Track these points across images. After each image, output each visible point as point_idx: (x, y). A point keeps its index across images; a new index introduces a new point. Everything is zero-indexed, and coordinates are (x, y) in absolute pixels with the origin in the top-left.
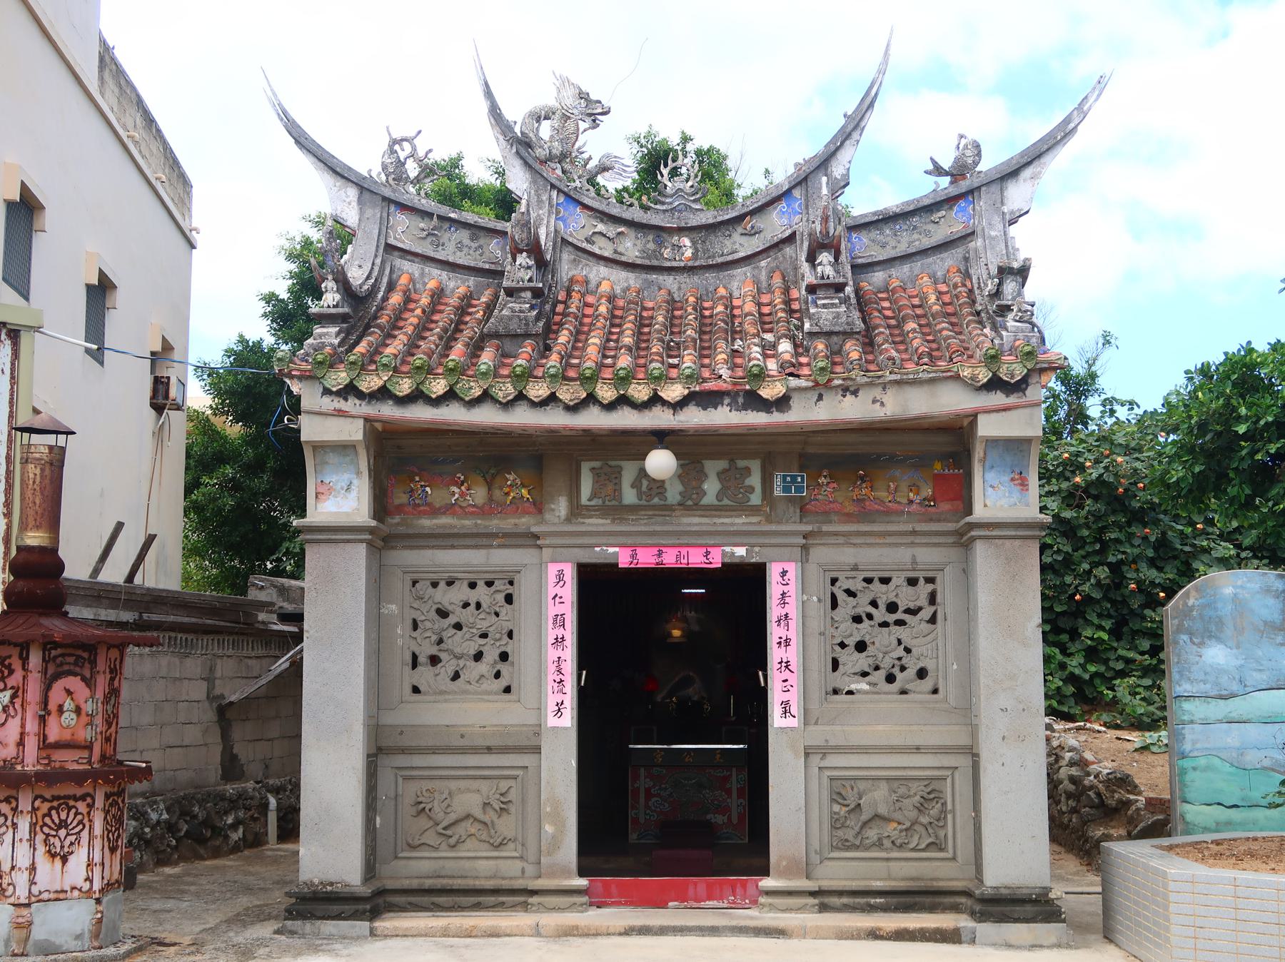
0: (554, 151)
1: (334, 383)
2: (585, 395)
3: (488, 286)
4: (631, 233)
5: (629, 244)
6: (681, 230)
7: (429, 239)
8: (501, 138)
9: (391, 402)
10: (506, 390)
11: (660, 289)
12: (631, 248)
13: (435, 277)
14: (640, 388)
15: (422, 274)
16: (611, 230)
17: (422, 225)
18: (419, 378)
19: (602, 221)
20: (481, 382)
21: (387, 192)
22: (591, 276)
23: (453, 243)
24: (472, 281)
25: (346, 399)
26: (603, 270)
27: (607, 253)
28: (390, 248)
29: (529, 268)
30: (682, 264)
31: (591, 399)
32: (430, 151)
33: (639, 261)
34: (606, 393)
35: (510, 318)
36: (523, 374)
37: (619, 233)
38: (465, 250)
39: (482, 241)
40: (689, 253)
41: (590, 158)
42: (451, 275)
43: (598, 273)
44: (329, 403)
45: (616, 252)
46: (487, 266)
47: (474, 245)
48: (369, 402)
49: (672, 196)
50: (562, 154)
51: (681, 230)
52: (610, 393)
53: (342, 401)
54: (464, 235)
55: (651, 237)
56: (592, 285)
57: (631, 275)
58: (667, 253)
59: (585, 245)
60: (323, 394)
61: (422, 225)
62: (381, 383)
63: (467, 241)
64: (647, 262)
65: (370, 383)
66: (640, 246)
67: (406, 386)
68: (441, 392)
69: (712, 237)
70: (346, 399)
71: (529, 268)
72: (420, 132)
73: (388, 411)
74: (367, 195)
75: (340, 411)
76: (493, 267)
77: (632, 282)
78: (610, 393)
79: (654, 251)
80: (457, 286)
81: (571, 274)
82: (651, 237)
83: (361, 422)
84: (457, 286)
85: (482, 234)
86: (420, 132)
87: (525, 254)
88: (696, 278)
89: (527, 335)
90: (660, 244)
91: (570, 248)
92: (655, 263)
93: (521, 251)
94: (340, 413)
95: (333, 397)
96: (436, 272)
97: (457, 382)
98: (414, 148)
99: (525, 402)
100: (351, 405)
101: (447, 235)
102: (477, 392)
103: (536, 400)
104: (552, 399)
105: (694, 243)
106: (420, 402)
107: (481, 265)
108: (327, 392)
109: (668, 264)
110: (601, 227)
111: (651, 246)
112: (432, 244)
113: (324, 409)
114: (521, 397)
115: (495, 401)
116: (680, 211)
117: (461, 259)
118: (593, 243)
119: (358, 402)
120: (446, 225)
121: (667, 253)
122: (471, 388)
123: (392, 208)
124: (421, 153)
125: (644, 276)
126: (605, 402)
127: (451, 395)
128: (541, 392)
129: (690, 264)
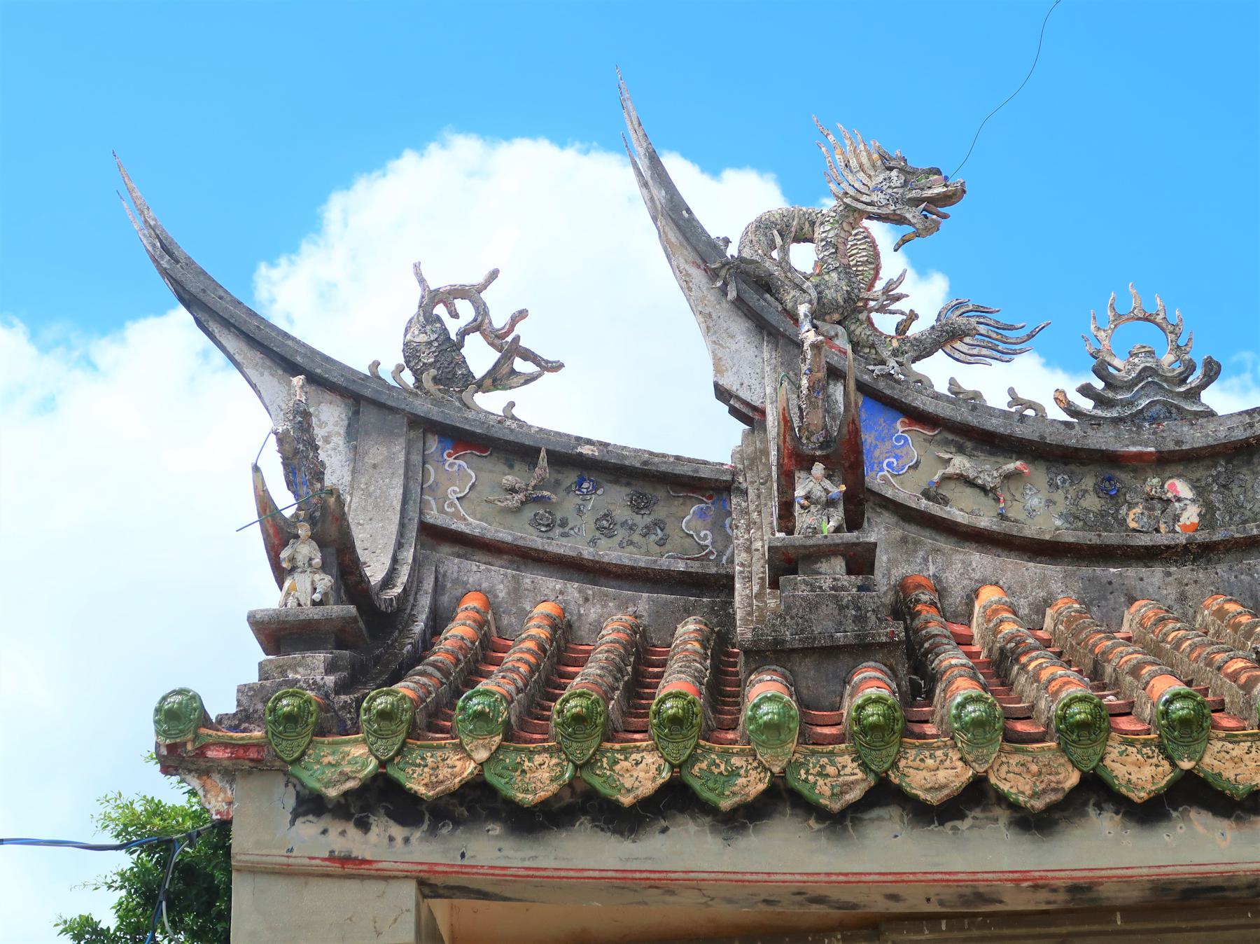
0: (829, 294)
1: (330, 774)
2: (1073, 779)
3: (687, 612)
4: (1038, 475)
5: (1035, 502)
6: (1167, 461)
7: (529, 513)
8: (698, 275)
9: (496, 829)
10: (838, 775)
11: (1131, 600)
12: (1041, 507)
13: (544, 600)
14: (1238, 750)
15: (516, 591)
16: (988, 470)
17: (509, 479)
18: (584, 749)
19: (961, 450)
20: (764, 756)
21: (422, 407)
22: (950, 577)
23: (589, 518)
24: (644, 602)
25: (364, 826)
26: (980, 561)
27: (985, 521)
28: (433, 535)
29: (830, 503)
30: (1182, 540)
31: (1096, 790)
32: (522, 314)
33: (1069, 537)
34: (1139, 772)
35: (813, 606)
36: (889, 719)
37: (1008, 477)
38: (621, 533)
39: (661, 512)
40: (1191, 515)
41: (913, 316)
42: (590, 590)
43: (963, 567)
44: (315, 839)
45: (1003, 517)
46: (681, 566)
47: (642, 521)
48: (433, 831)
49: (1130, 385)
50: (849, 299)
51: (1167, 461)
52: (1148, 771)
53: (353, 832)
54: (615, 499)
55: (1089, 482)
56: (955, 598)
57: (1054, 573)
58: (1134, 517)
59: (924, 504)
60: (296, 814)
61: (509, 479)
62: (470, 767)
63: (622, 513)
64: (1091, 538)
65: (438, 769)
66: (1062, 505)
67: (544, 775)
68: (647, 787)
69: (1246, 475)
70: (364, 826)
71: (830, 503)
72: (494, 275)
73: (488, 850)
74: (370, 416)
75: (346, 860)
76: (695, 567)
77: (1056, 587)
78: (1148, 771)
79: (1102, 514)
80: (610, 620)
81: (898, 573)
82: (1089, 482)
83: (408, 891)
84: (610, 620)
85: (660, 494)
86: (494, 275)
87: (818, 469)
88: (1222, 569)
89: (863, 649)
90: (1112, 495)
91: (887, 518)
92: (1112, 538)
93: (806, 463)
94: (348, 867)
95: (325, 822)
96: (551, 584)
97: (692, 759)
98: (482, 310)
99: (894, 812)
100: (382, 841)
101: (574, 500)
102: (753, 785)
103: (933, 798)
104: (977, 795)
105: (1200, 491)
106: (584, 822)
107: (664, 563)
108: (310, 804)
109: (1144, 540)
110: (960, 464)
111: (1092, 502)
112: (535, 522)
113: (299, 860)
114: (885, 793)
115: (806, 807)
116: (1153, 420)
117: (610, 552)
118: (945, 501)
119: (398, 831)
120: (570, 478)
121: (1134, 517)
122: (734, 773)
123: (433, 444)
124: (499, 320)
125: (1086, 571)
126: (1139, 796)
127: (676, 799)
128: (942, 776)
129: (1202, 537)
